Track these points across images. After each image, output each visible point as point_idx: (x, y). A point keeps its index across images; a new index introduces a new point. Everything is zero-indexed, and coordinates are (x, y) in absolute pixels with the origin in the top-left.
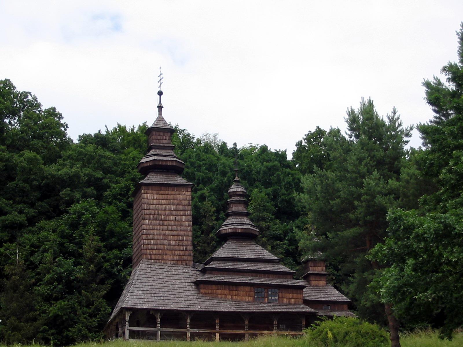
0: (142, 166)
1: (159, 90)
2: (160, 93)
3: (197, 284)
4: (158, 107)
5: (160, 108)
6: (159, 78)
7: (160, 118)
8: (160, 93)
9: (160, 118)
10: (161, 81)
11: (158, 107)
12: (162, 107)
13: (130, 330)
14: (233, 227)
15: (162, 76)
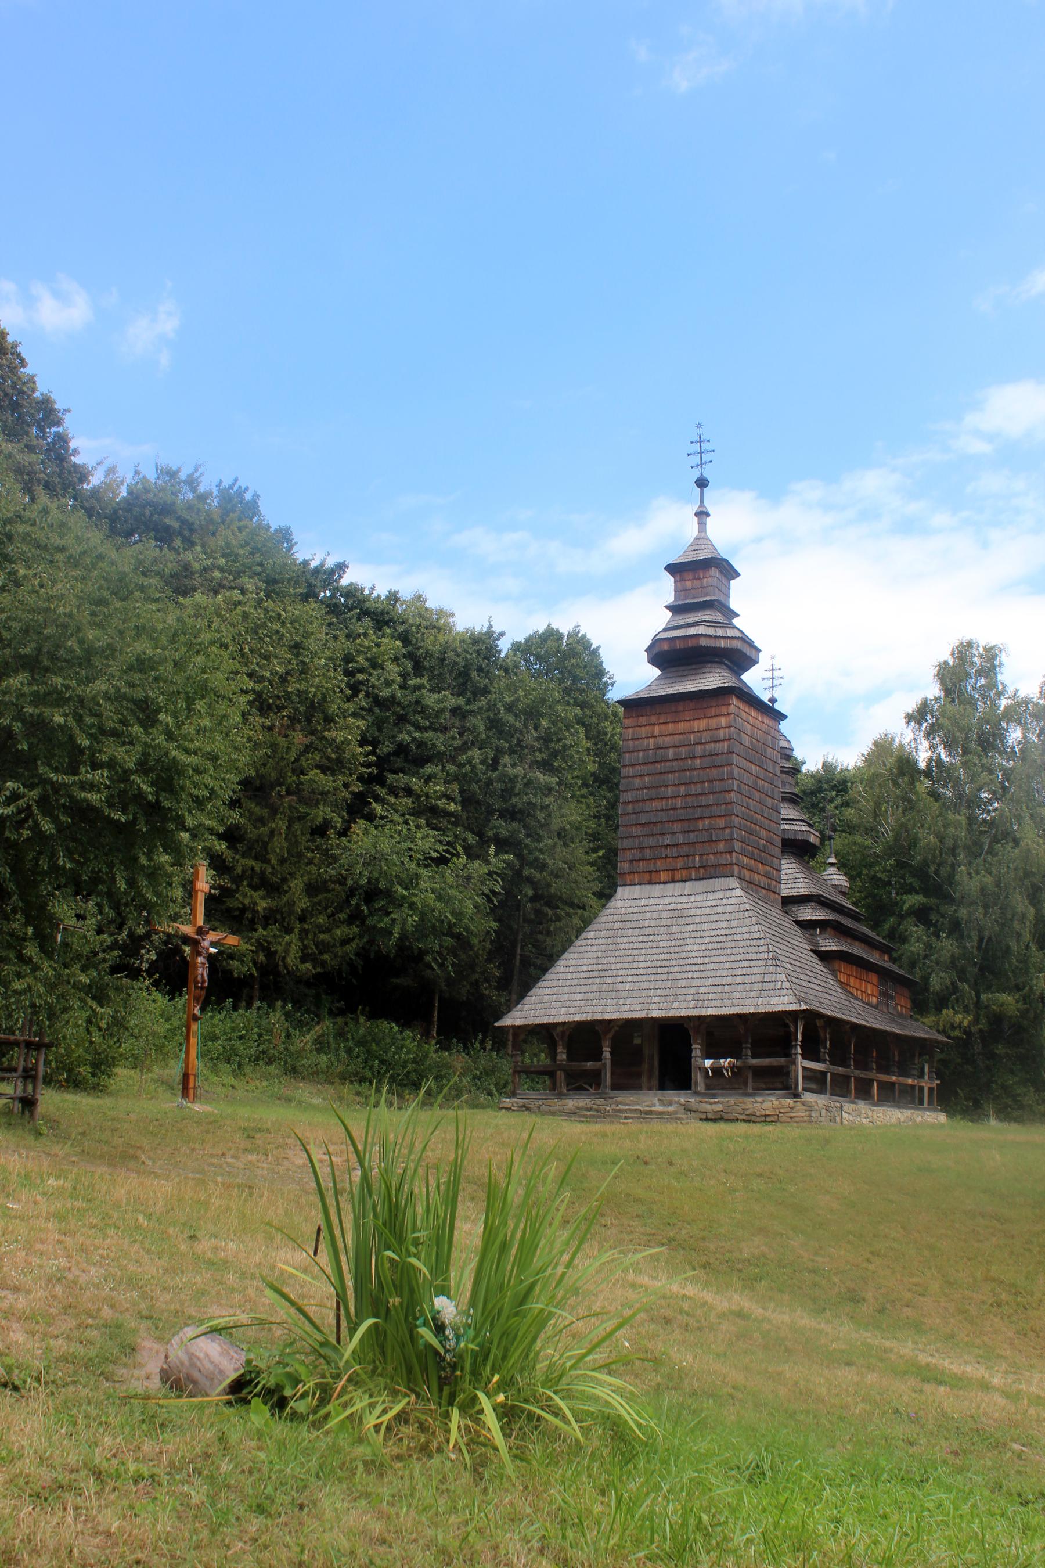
0: (703, 642)
1: (696, 474)
2: (702, 483)
3: (824, 957)
4: (697, 514)
5: (702, 514)
6: (696, 447)
7: (701, 539)
8: (702, 483)
9: (701, 539)
10: (705, 457)
11: (697, 514)
12: (708, 515)
13: (804, 1068)
14: (804, 828)
15: (705, 446)
